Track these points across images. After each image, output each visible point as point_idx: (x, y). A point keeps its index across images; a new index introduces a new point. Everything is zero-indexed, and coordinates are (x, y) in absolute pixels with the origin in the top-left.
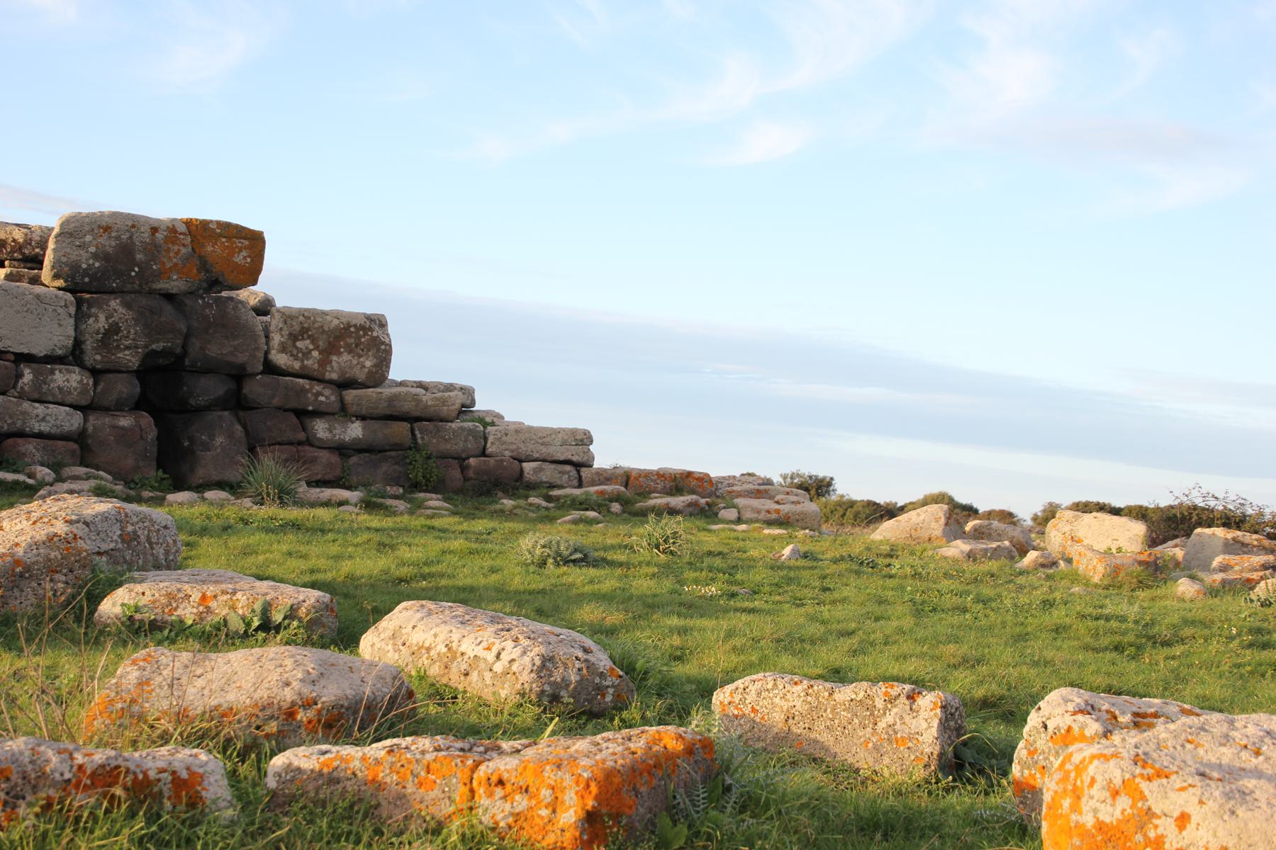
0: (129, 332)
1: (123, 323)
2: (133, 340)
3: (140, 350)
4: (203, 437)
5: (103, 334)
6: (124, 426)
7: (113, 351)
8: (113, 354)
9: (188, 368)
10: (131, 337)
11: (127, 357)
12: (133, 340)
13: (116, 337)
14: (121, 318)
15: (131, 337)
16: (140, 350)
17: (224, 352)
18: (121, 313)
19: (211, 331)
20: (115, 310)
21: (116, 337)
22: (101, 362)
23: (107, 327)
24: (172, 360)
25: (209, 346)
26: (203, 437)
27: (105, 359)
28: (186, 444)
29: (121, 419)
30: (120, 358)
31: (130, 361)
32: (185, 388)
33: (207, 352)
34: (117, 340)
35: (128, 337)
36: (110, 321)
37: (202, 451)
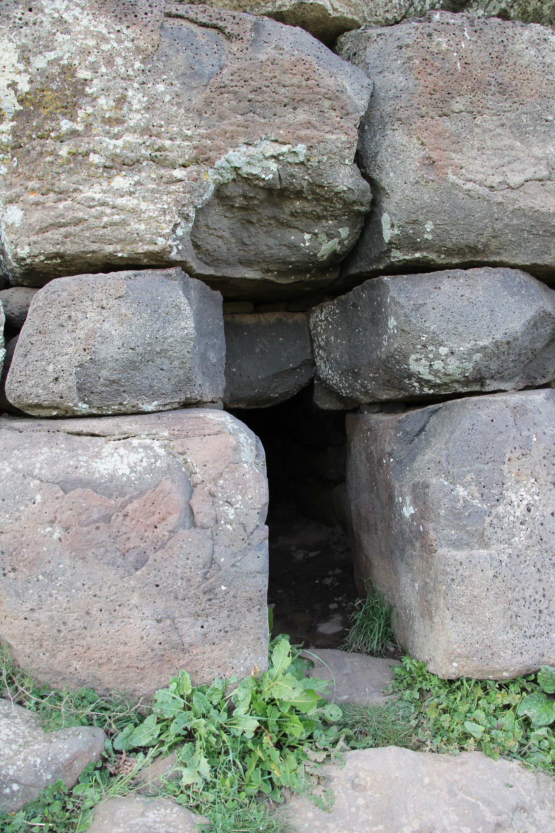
0: (121, 101)
1: (93, 67)
2: (146, 131)
3: (178, 173)
4: (461, 491)
5: (18, 115)
6: (112, 478)
7: (64, 183)
8: (63, 194)
9: (398, 256)
10: (134, 119)
11: (120, 201)
12: (146, 131)
13: (65, 125)
14: (85, 52)
15: (134, 119)
16: (178, 173)
17: (515, 179)
18: (87, 32)
19: (458, 105)
20: (61, 21)
21: (65, 125)
22: (27, 229)
23: (24, 87)
24: (344, 232)
25: (456, 158)
26: (461, 491)
27: (37, 216)
28: (408, 511)
29: (108, 447)
30: (90, 204)
31: (133, 211)
32: (392, 322)
33: (452, 178)
34: (74, 133)
35: (119, 121)
36: (40, 62)
37: (457, 545)
